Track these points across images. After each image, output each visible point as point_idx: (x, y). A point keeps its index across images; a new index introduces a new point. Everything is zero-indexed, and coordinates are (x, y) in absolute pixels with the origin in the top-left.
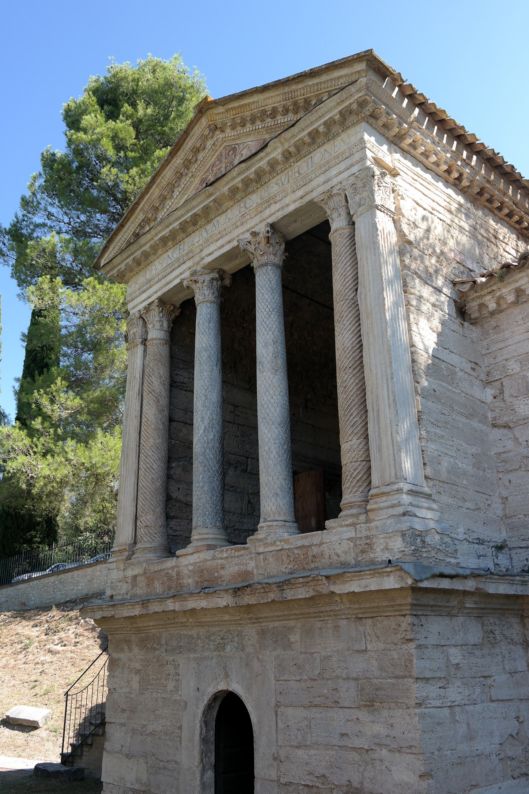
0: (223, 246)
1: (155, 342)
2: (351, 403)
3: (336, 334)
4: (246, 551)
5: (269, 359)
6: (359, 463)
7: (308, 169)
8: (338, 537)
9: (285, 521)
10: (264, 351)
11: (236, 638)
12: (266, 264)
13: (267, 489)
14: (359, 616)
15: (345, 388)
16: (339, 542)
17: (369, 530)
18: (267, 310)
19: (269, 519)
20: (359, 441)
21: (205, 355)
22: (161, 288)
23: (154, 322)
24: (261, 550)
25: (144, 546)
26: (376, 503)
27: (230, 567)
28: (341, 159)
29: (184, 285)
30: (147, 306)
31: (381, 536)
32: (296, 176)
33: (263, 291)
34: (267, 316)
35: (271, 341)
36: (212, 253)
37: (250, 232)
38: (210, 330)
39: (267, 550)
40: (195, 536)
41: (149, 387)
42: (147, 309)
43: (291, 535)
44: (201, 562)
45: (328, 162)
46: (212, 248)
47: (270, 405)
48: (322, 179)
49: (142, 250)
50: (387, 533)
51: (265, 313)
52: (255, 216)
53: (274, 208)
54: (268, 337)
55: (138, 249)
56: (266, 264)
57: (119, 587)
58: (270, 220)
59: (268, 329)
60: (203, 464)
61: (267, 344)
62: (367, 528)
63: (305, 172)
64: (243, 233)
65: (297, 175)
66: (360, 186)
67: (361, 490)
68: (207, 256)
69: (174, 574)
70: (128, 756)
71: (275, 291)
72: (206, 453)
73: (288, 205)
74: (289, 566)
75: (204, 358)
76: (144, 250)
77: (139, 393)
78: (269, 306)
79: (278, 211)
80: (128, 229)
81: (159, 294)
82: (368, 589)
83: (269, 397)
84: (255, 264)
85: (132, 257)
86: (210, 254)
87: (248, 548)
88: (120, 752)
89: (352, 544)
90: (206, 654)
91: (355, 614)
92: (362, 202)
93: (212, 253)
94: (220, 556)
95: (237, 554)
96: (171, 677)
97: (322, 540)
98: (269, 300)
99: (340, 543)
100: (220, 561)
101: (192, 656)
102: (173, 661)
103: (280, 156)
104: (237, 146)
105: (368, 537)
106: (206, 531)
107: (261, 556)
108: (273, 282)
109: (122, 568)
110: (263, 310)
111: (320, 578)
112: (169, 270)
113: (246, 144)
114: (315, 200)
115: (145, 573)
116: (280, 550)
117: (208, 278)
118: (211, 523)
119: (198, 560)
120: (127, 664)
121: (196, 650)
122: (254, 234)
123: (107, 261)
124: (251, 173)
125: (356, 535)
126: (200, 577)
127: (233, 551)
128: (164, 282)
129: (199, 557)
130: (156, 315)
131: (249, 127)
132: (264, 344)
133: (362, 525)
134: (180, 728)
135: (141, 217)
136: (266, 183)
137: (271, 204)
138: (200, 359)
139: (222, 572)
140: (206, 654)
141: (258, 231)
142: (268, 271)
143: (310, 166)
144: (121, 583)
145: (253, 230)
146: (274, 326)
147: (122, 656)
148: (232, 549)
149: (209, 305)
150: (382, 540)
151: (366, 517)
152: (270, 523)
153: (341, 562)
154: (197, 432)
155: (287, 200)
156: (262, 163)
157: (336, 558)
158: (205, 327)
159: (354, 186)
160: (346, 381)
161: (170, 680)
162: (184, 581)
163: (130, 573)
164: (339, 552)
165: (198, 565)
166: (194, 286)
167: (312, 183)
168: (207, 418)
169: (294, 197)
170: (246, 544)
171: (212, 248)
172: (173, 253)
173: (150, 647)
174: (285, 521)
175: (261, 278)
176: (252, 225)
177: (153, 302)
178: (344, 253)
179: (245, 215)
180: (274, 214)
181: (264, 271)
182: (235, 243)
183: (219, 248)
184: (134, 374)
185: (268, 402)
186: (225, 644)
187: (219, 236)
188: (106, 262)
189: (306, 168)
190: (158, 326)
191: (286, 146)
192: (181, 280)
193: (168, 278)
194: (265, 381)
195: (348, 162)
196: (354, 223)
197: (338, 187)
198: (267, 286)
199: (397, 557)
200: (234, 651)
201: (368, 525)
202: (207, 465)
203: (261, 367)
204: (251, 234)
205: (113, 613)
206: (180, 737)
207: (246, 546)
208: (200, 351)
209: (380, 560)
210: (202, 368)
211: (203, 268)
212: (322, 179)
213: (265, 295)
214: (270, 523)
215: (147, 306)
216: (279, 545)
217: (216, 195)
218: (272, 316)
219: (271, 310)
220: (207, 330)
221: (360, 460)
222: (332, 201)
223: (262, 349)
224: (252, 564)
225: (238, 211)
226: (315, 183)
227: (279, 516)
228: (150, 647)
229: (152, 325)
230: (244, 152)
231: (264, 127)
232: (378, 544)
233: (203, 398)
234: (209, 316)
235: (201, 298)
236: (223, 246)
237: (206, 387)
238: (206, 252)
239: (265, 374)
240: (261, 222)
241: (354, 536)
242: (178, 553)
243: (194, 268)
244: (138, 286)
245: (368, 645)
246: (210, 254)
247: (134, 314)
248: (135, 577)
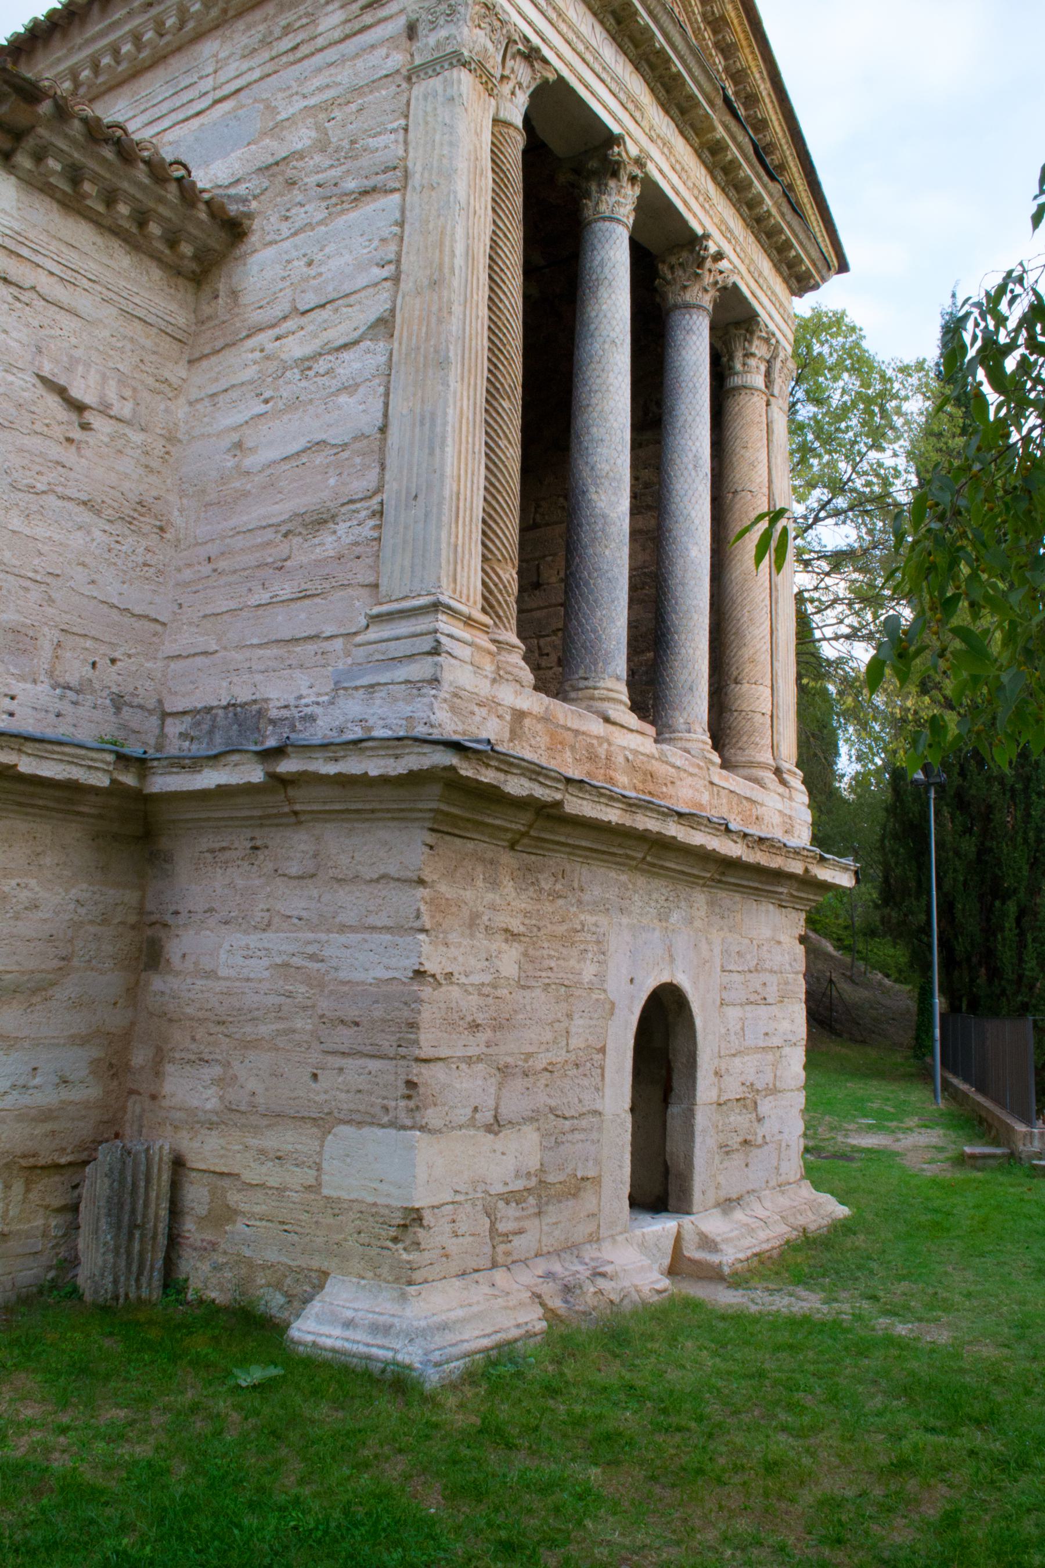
70: (488, 1129)
88: (472, 1123)
96: (590, 955)
102: (596, 925)
120: (485, 918)
124: (745, 171)
134: (603, 1050)
136: (727, 195)
144: (484, 711)
147: (468, 895)
156: (756, 182)
161: (588, 962)
173: (547, 888)
191: (774, 211)
205: (558, 796)
206: (602, 1068)
228: (547, 888)
236: (677, 193)
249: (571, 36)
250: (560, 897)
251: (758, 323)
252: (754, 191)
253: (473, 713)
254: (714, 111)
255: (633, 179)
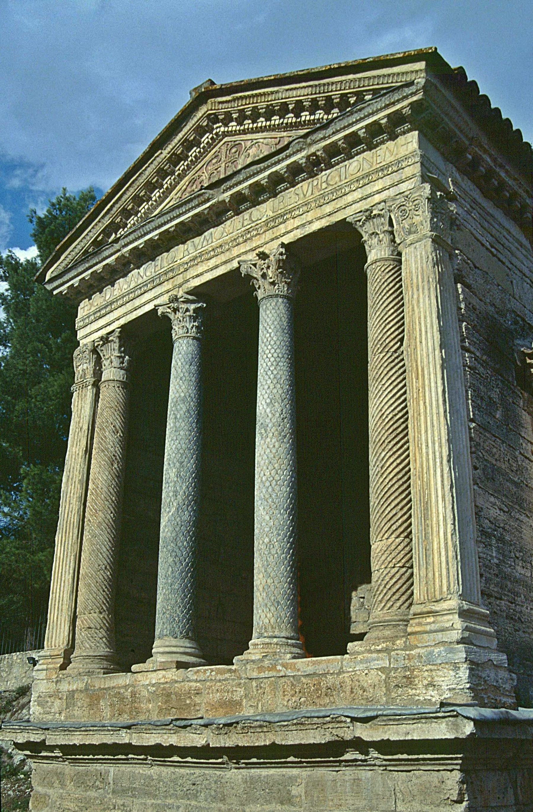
0: (217, 267)
1: (112, 384)
2: (389, 489)
3: (371, 395)
4: (233, 674)
5: (274, 420)
6: (396, 569)
7: (340, 181)
8: (365, 665)
9: (287, 638)
10: (268, 410)
11: (213, 785)
12: (277, 296)
13: (265, 594)
14: (389, 768)
15: (382, 468)
16: (366, 671)
17: (409, 659)
18: (275, 355)
19: (266, 634)
20: (398, 540)
21: (184, 408)
22: (126, 314)
23: (112, 357)
24: (255, 675)
25: (85, 654)
26: (420, 624)
27: (208, 693)
28: (385, 172)
29: (159, 313)
30: (105, 336)
31: (425, 668)
32: (323, 187)
33: (270, 331)
34: (274, 363)
35: (278, 396)
36: (202, 274)
37: (257, 251)
38: (191, 375)
39: (262, 675)
40: (158, 647)
41: (101, 444)
42: (105, 340)
43: (294, 658)
44: (167, 682)
45: (368, 175)
46: (200, 269)
47: (274, 483)
48: (357, 195)
49: (104, 263)
50: (433, 665)
51: (272, 359)
52: (265, 232)
53: (291, 224)
54: (275, 391)
55: (100, 262)
56: (277, 296)
57: (49, 704)
58: (286, 240)
59: (275, 381)
60: (174, 554)
61: (273, 401)
62: (406, 657)
63: (336, 183)
64: (246, 253)
65: (324, 185)
66: (410, 208)
67: (398, 604)
68: (193, 278)
69: (128, 694)
71: (286, 331)
72: (178, 539)
73: (310, 222)
74: (294, 699)
75: (182, 412)
76: (107, 264)
77: (86, 451)
78: (278, 351)
79: (297, 228)
80: (87, 235)
81: (122, 322)
82: (409, 737)
83: (273, 472)
84: (260, 294)
85: (90, 271)
86: (197, 276)
87: (235, 671)
89: (384, 677)
90: (170, 801)
91: (383, 766)
92: (413, 229)
93: (202, 274)
94: (195, 677)
95: (219, 677)
97: (342, 668)
98: (278, 343)
99: (366, 674)
100: (194, 684)
101: (150, 802)
102: (123, 805)
103: (304, 160)
104: (243, 143)
105: (406, 668)
106: (174, 642)
107: (254, 684)
108: (283, 319)
109: (55, 680)
110: (270, 356)
111: (343, 719)
112: (139, 292)
113: (255, 141)
114: (348, 220)
115: (87, 689)
116: (282, 677)
117: (192, 307)
118: (181, 633)
119: (162, 681)
121: (156, 795)
122: (263, 256)
123: (55, 274)
124: (264, 178)
125: (390, 664)
126: (166, 702)
127: (213, 673)
128: (129, 306)
129: (164, 677)
130: (117, 348)
131: (262, 122)
132: (268, 401)
133: (399, 652)
135: (107, 221)
137: (287, 219)
138: (176, 412)
139: (197, 700)
140: (170, 801)
141: (267, 252)
142: (279, 304)
143: (343, 177)
144: (52, 699)
145: (261, 250)
146: (284, 378)
147: (50, 791)
148: (212, 671)
149: (191, 342)
150: (426, 673)
151: (405, 642)
152: (267, 640)
153: (367, 699)
154: (168, 510)
155: (309, 216)
157: (361, 692)
158: (184, 370)
159: (403, 208)
160: (383, 459)
162: (142, 705)
163: (65, 687)
164: (365, 685)
165: (162, 686)
166: (172, 316)
167: (345, 197)
168: (181, 492)
169: (319, 212)
170: (233, 664)
171: (200, 269)
172: (145, 270)
173: (91, 785)
174: (287, 638)
175: (268, 312)
176: (259, 243)
177: (113, 331)
178: (385, 291)
179: (251, 230)
180: (291, 231)
181: (274, 303)
182: (235, 264)
183: (212, 269)
184: (81, 425)
185: (272, 479)
186: (197, 792)
187: (212, 253)
188: (53, 275)
189: (337, 179)
190: (116, 363)
191: (313, 149)
192: (155, 306)
193: (137, 302)
194: (268, 450)
195: (396, 177)
196: (400, 254)
197: (380, 206)
198: (276, 323)
199: (445, 696)
200: (209, 800)
201: (407, 652)
202: (179, 554)
203: (263, 431)
204: (257, 255)
207: (233, 667)
208: (177, 401)
209: (421, 698)
210: (178, 424)
211: (187, 293)
212: (357, 195)
213: (272, 335)
214: (267, 640)
215: (105, 336)
216: (280, 671)
217: (214, 201)
218: (281, 364)
219: (280, 355)
220: (186, 374)
221: (398, 565)
222: (371, 223)
223: (265, 407)
224: (241, 691)
225: (241, 224)
226: (350, 198)
227: (280, 630)
228: (91, 785)
229: (109, 360)
230: (252, 151)
231: (282, 123)
232: (420, 678)
233: (178, 465)
234: (190, 356)
235: (181, 331)
236: (217, 267)
237: (181, 451)
238: (192, 272)
239: (268, 440)
240: (273, 240)
241: (388, 666)
242: (134, 668)
243: (174, 292)
244: (93, 309)
245: (398, 804)
246: (197, 276)
247: (85, 345)
248: (72, 694)
249: (120, 302)
250: (100, 789)
251: (348, 222)
252: (282, 172)
253: (47, 702)
254: (212, 198)
255: (175, 310)
